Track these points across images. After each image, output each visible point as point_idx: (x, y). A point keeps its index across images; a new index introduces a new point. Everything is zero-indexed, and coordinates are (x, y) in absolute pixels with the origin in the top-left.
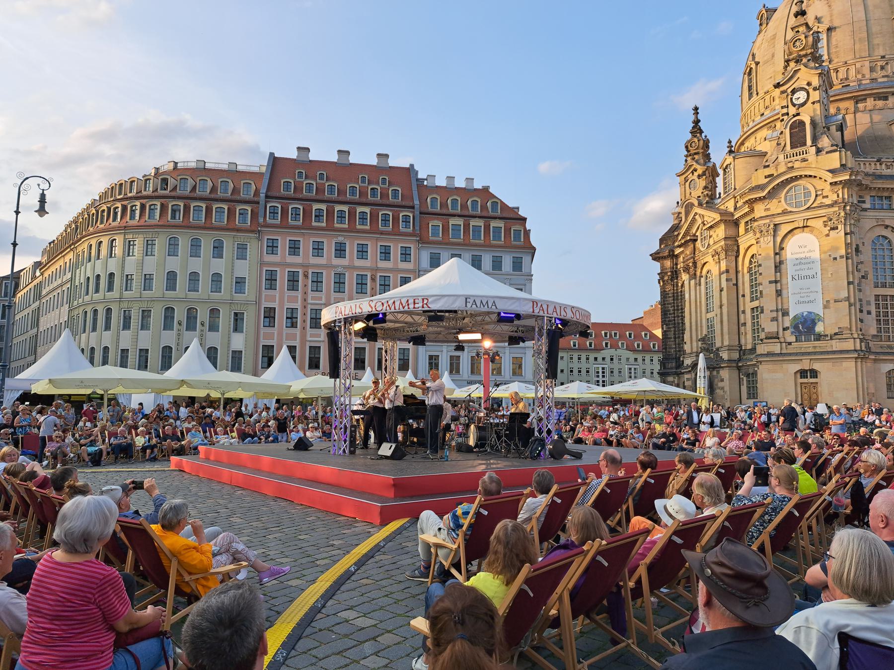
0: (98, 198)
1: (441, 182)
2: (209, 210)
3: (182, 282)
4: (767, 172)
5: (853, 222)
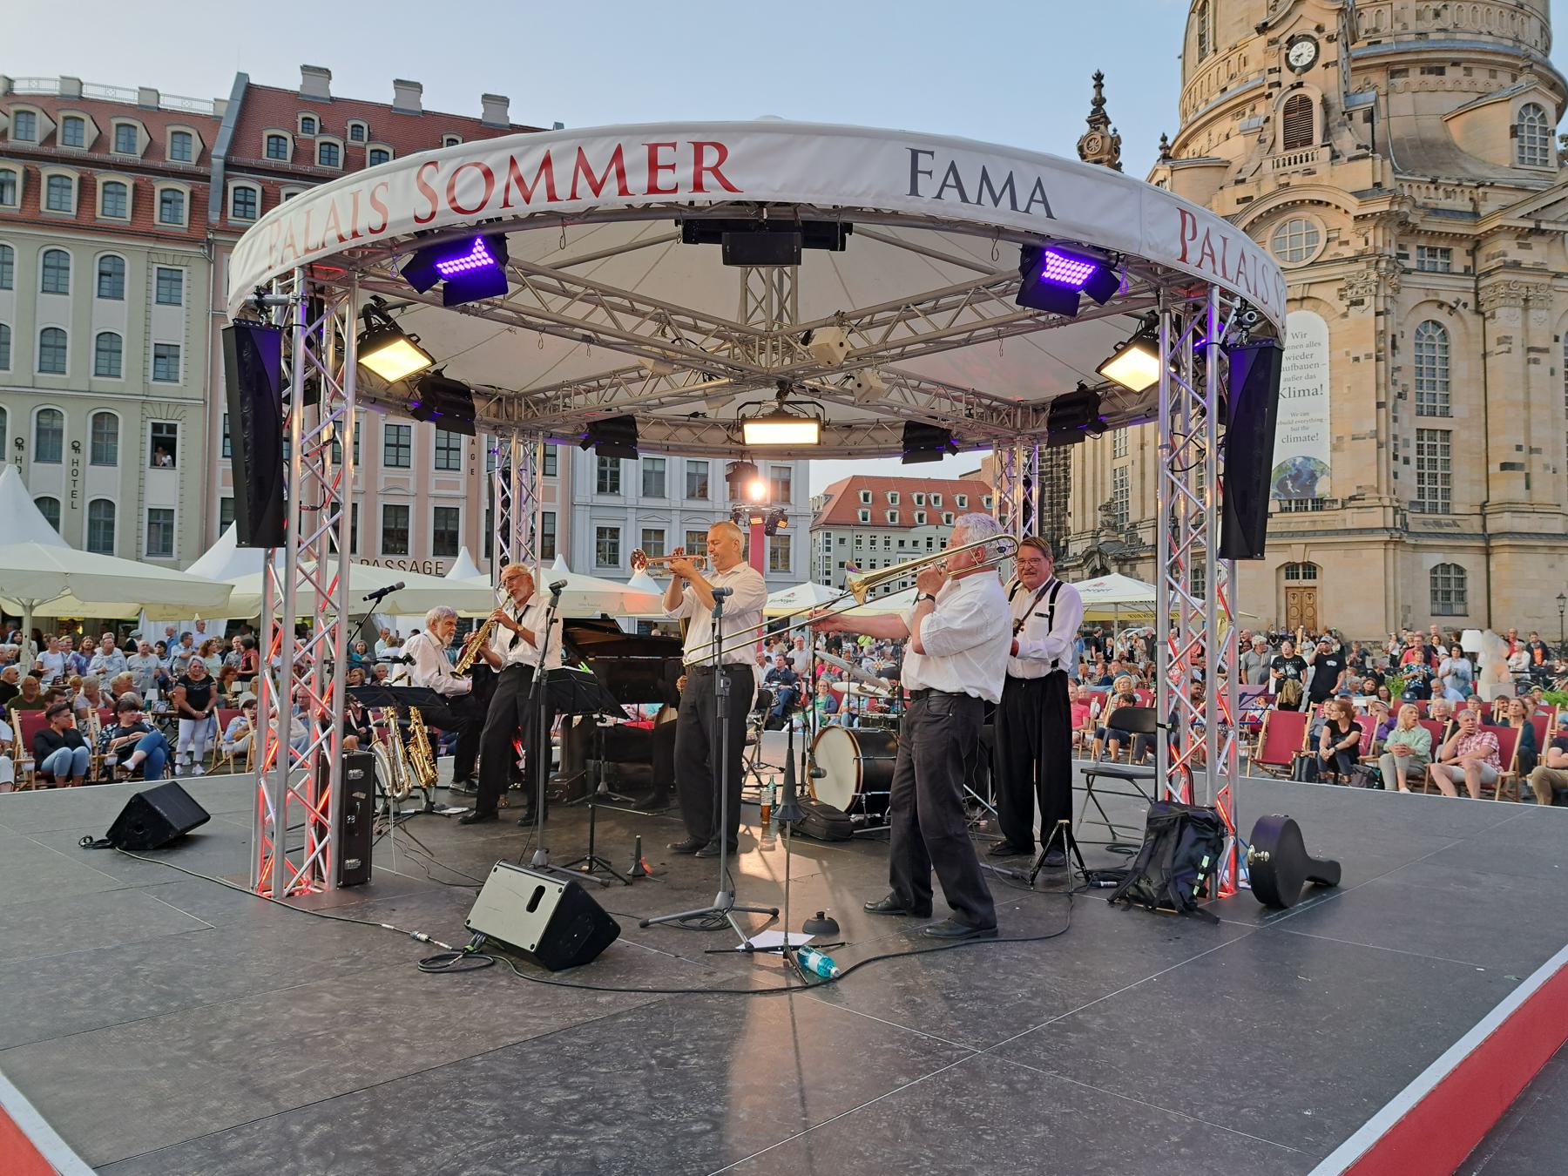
2: (86, 188)
4: (1242, 191)
5: (1389, 291)
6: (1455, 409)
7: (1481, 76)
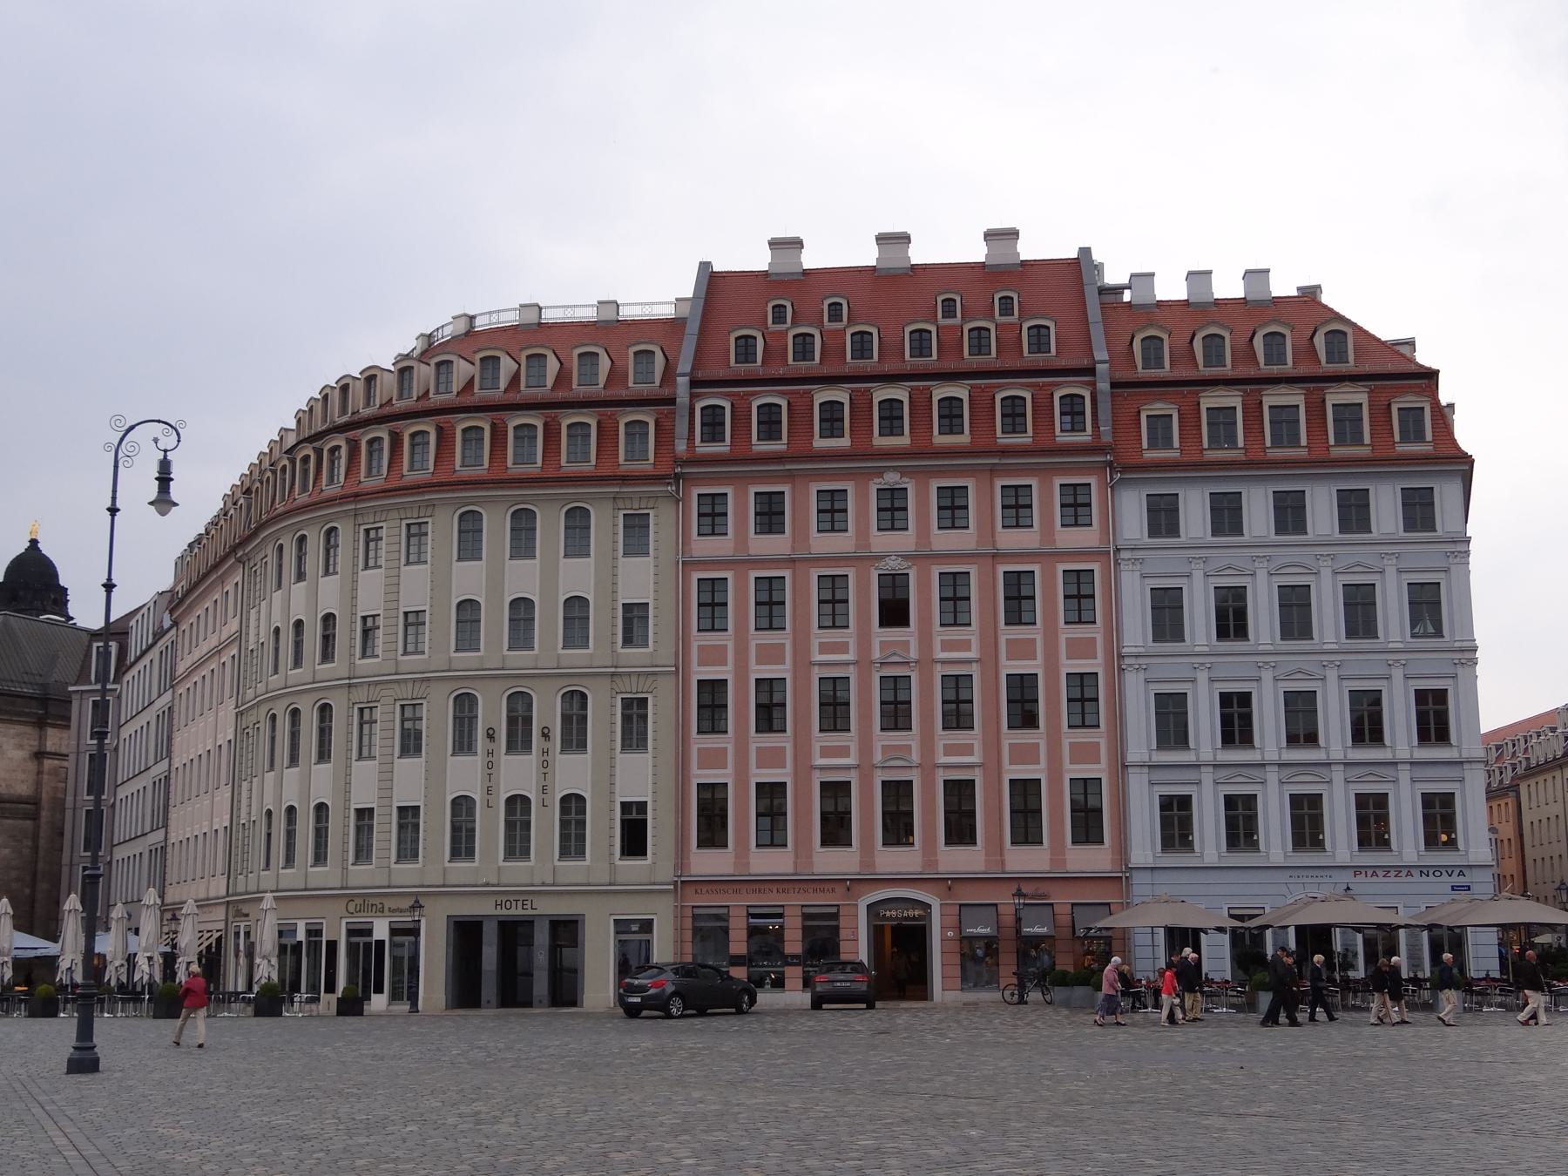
0: (293, 425)
1: (1170, 288)
3: (495, 624)
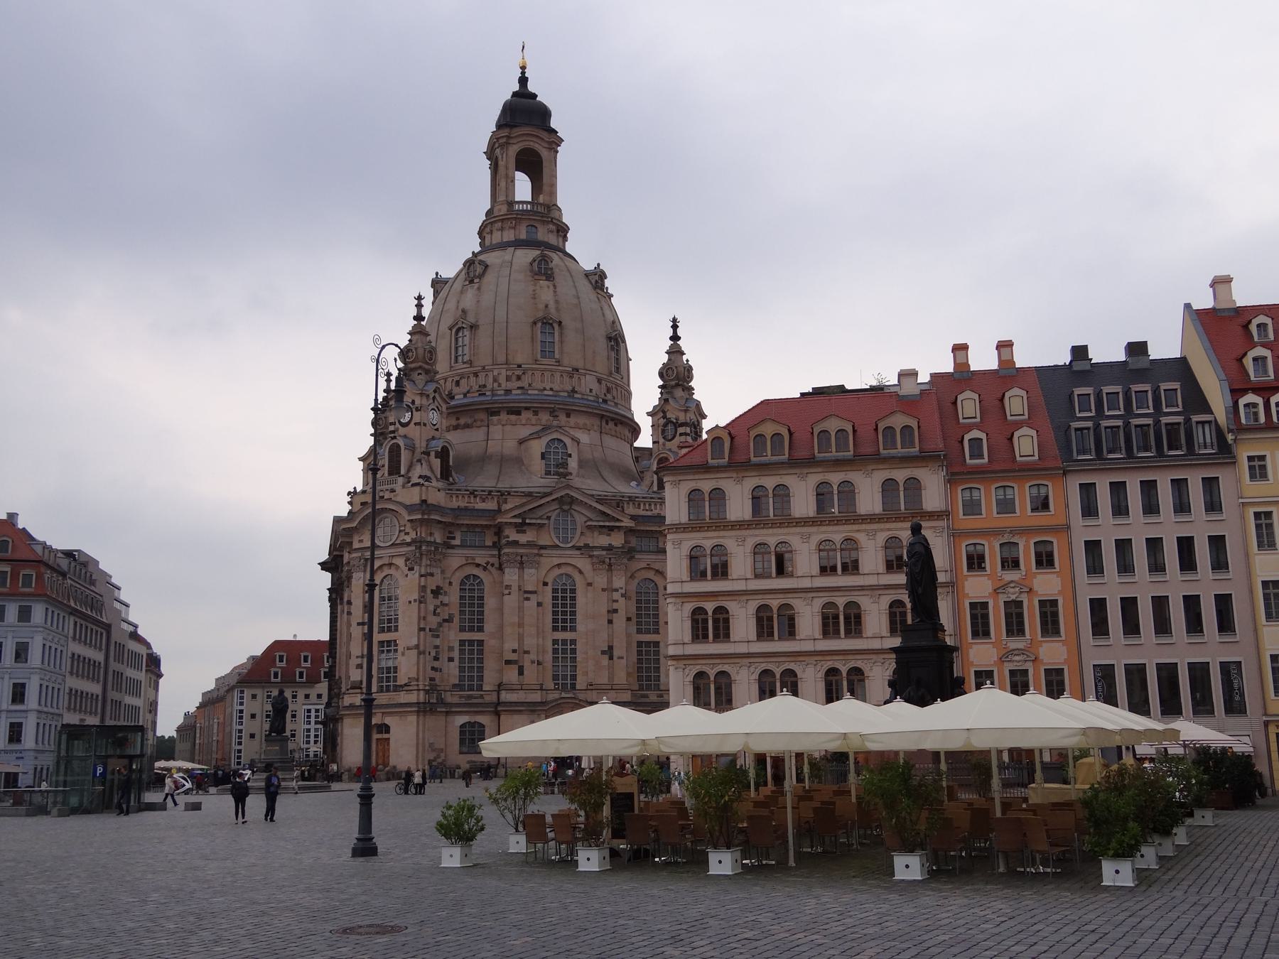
6: (489, 626)
7: (545, 418)
